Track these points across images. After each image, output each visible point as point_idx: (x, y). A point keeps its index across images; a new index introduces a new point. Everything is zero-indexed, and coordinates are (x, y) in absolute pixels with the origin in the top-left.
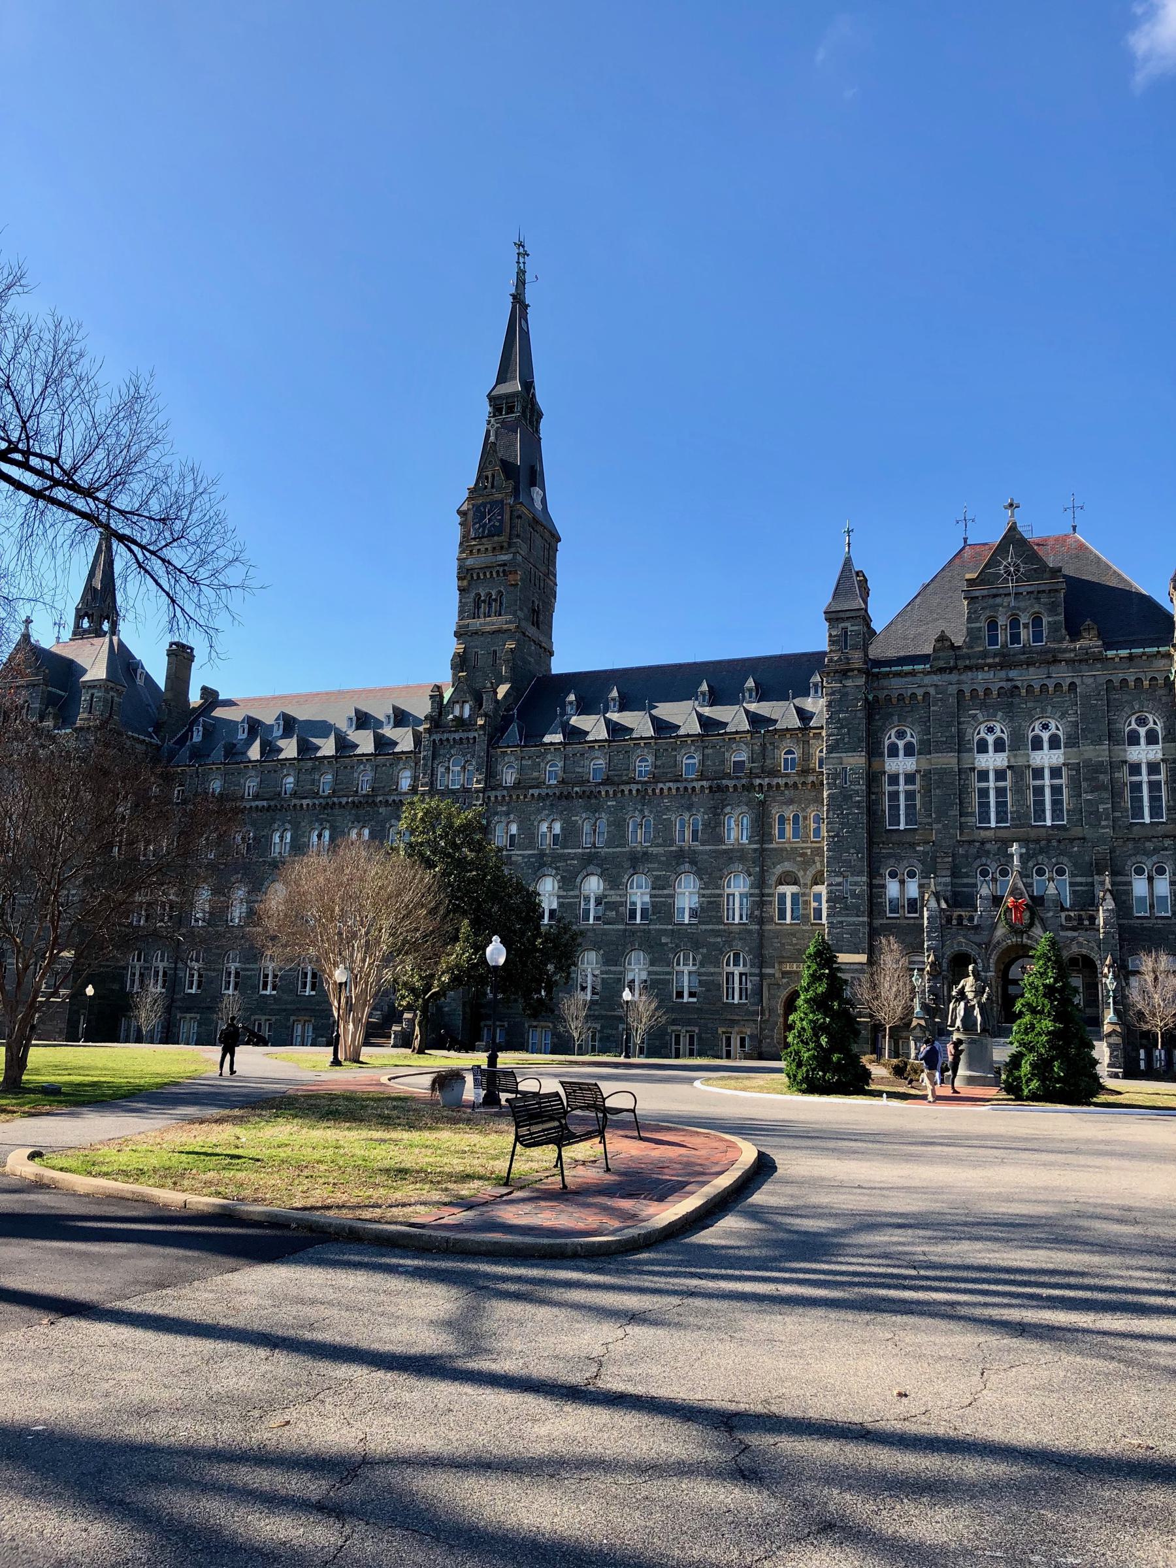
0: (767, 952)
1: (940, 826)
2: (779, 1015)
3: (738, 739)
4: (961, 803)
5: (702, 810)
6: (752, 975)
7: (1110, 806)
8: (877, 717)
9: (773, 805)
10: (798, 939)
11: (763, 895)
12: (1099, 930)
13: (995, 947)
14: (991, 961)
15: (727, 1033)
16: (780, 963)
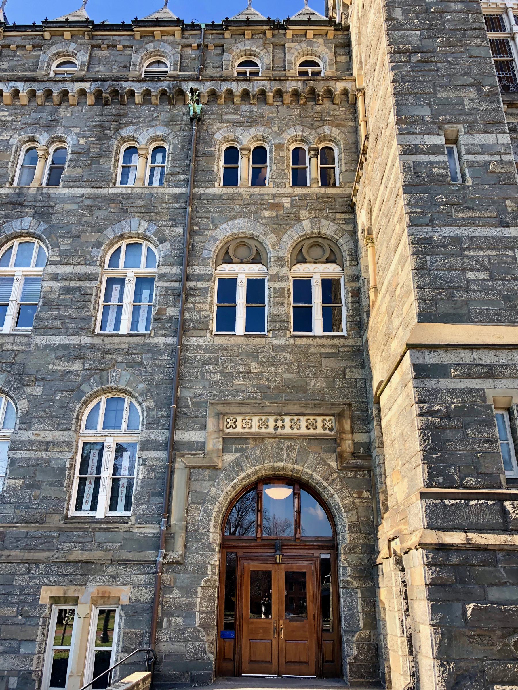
0: (187, 394)
2: (209, 547)
3: (157, 34)
5: (76, 130)
6: (146, 446)
9: (217, 125)
10: (262, 364)
11: (188, 278)
15: (66, 600)
16: (221, 415)
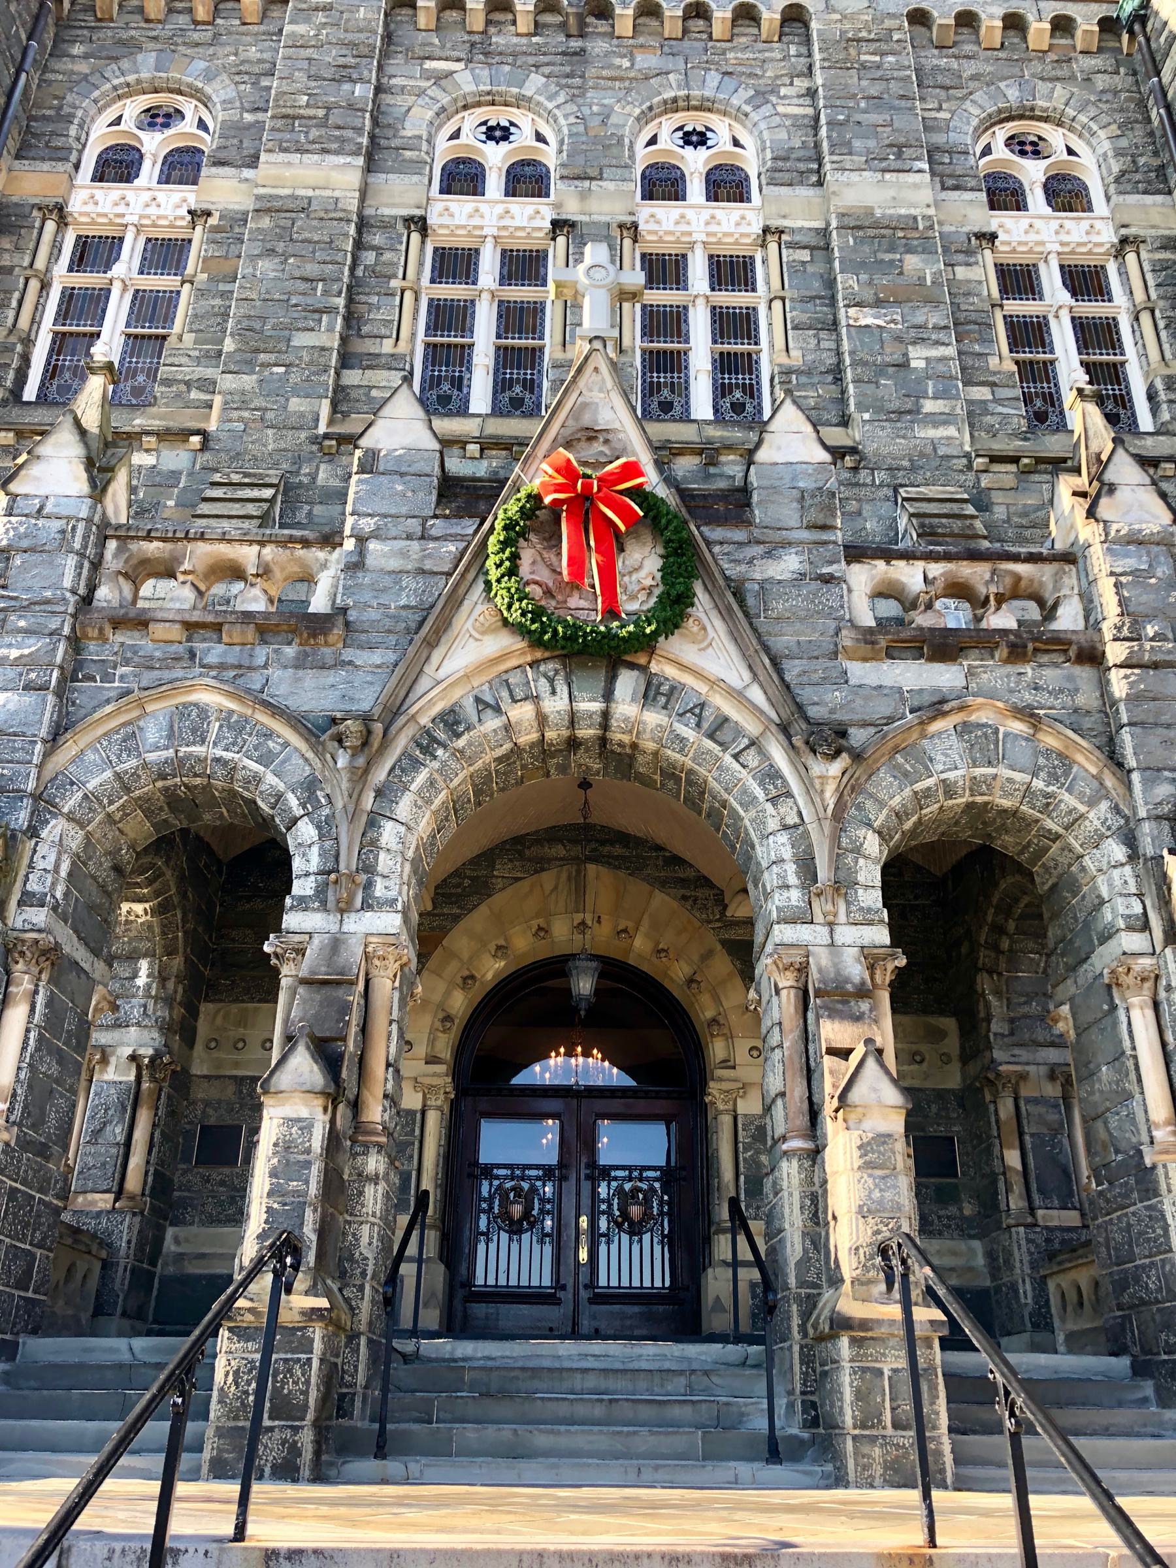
1: (248, 381)
4: (352, 319)
7: (951, 351)
8: (77, 49)
12: (1092, 657)
13: (427, 744)
14: (389, 833)
